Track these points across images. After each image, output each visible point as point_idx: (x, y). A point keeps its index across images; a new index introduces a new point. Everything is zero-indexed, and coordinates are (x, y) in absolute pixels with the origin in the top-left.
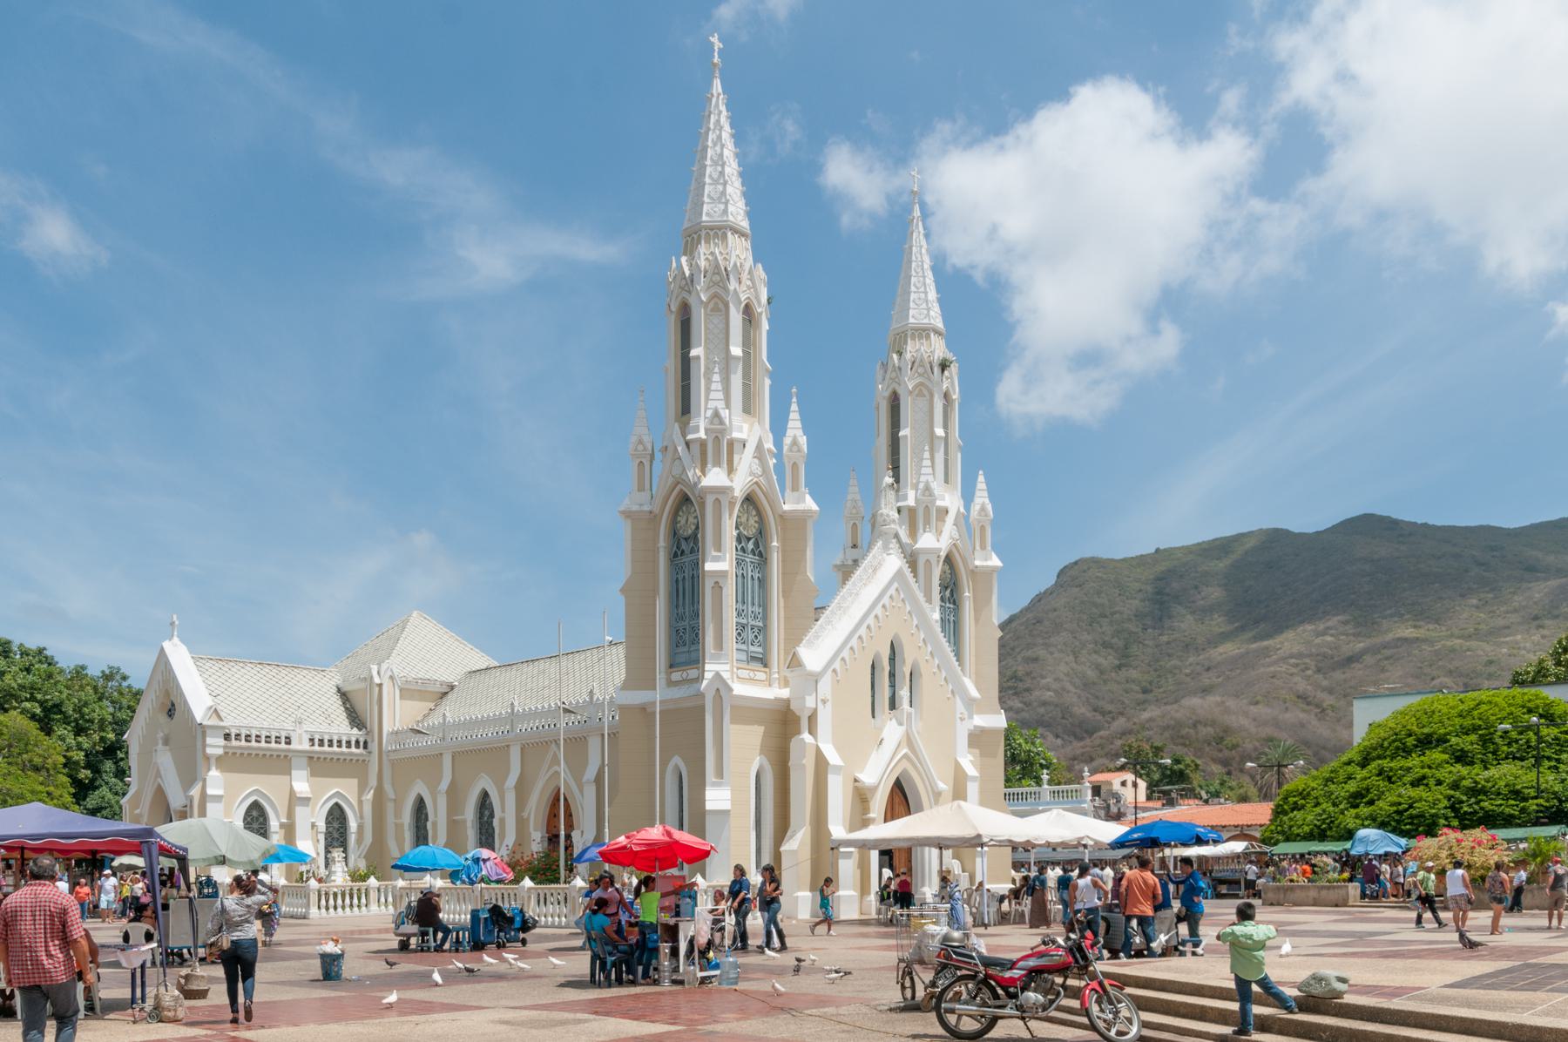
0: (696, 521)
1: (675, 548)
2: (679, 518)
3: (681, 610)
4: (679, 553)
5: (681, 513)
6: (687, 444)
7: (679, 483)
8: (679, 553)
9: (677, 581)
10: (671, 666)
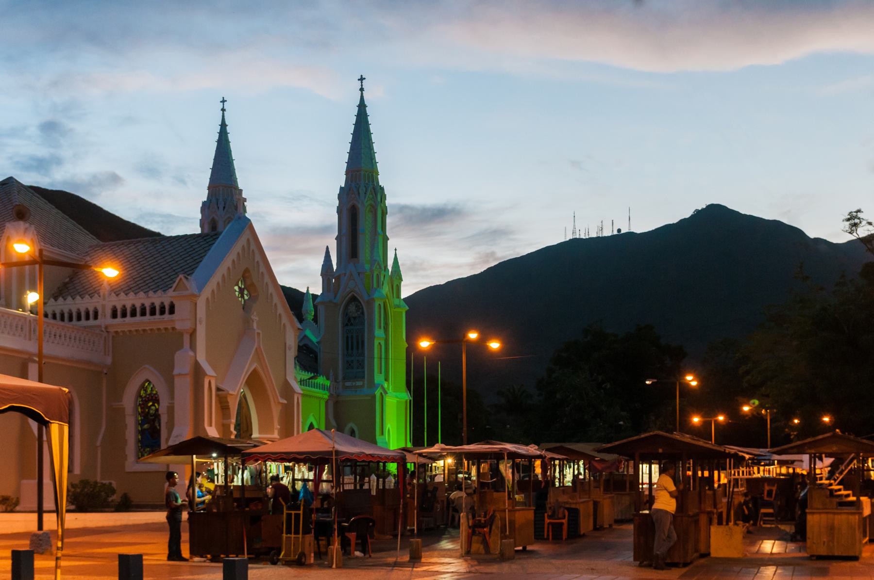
3: (350, 351)
4: (349, 324)
7: (352, 291)
9: (347, 337)
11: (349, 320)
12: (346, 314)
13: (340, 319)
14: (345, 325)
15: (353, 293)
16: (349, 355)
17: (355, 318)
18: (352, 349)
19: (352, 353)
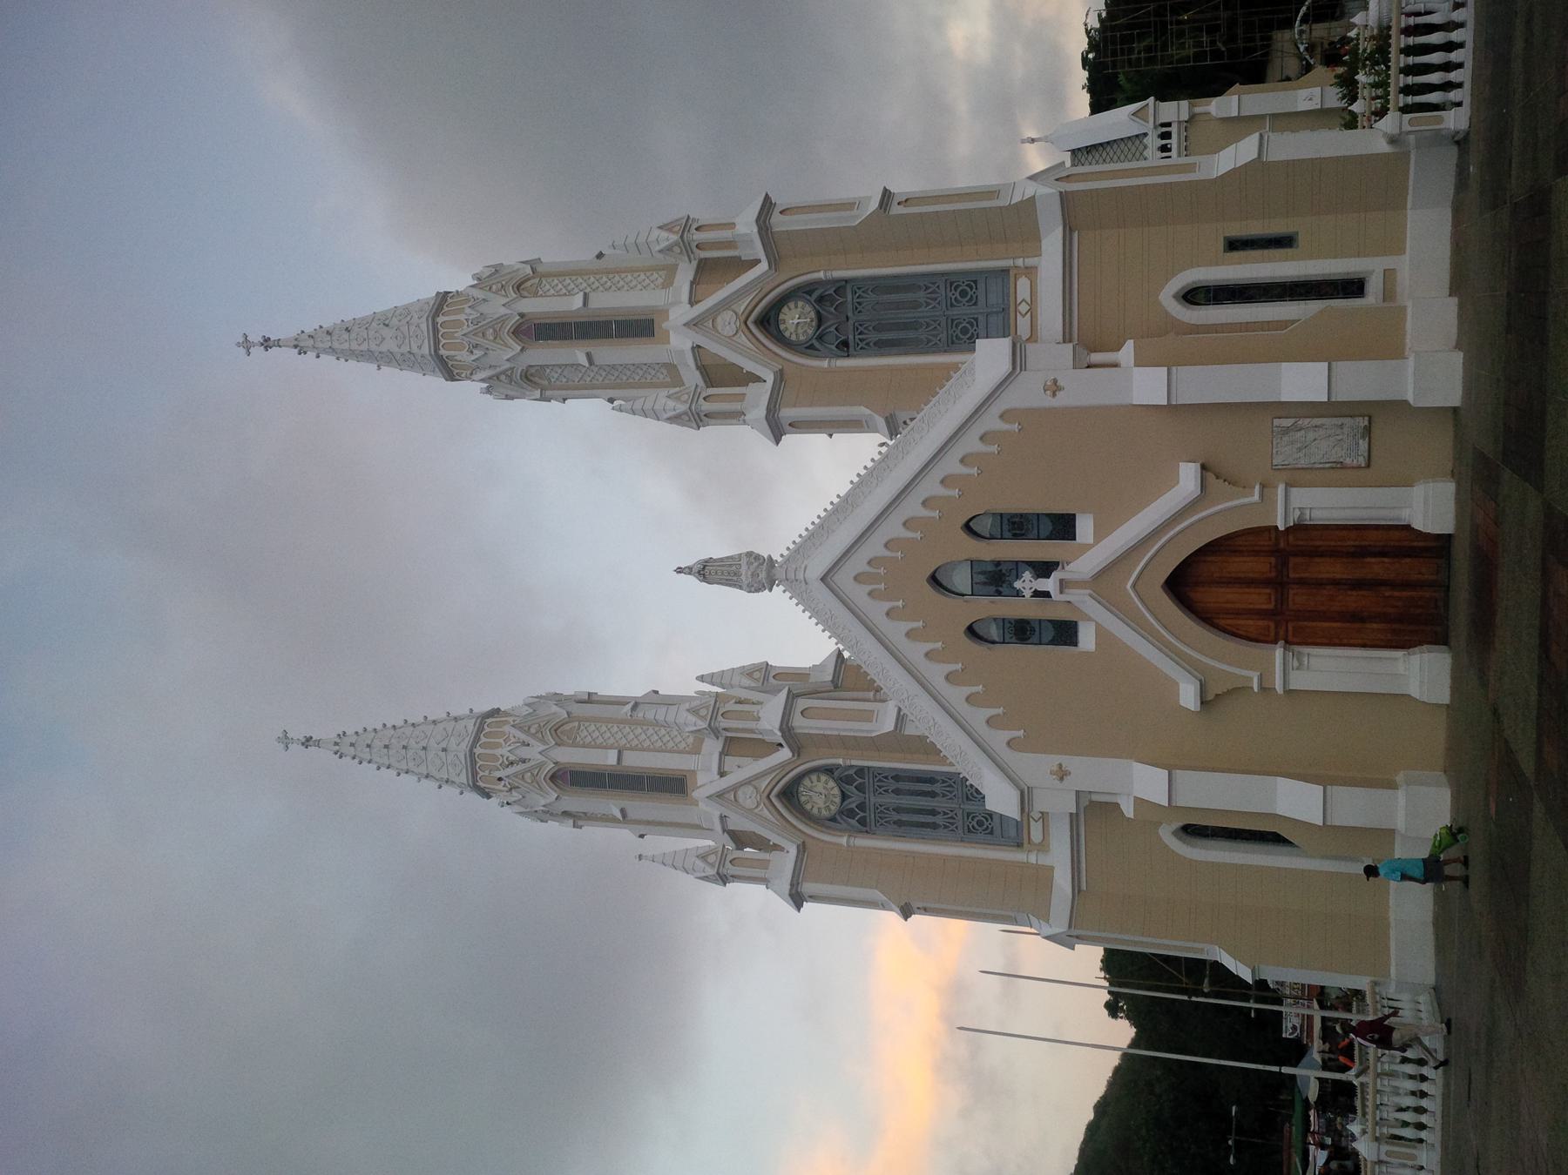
0: (823, 778)
1: (853, 822)
2: (815, 811)
3: (939, 819)
4: (862, 814)
5: (808, 807)
6: (722, 774)
8: (862, 814)
9: (900, 823)
10: (1019, 845)
11: (850, 813)
12: (831, 822)
13: (844, 840)
14: (864, 826)
15: (772, 797)
16: (952, 824)
17: (844, 796)
18: (933, 812)
19: (945, 814)
